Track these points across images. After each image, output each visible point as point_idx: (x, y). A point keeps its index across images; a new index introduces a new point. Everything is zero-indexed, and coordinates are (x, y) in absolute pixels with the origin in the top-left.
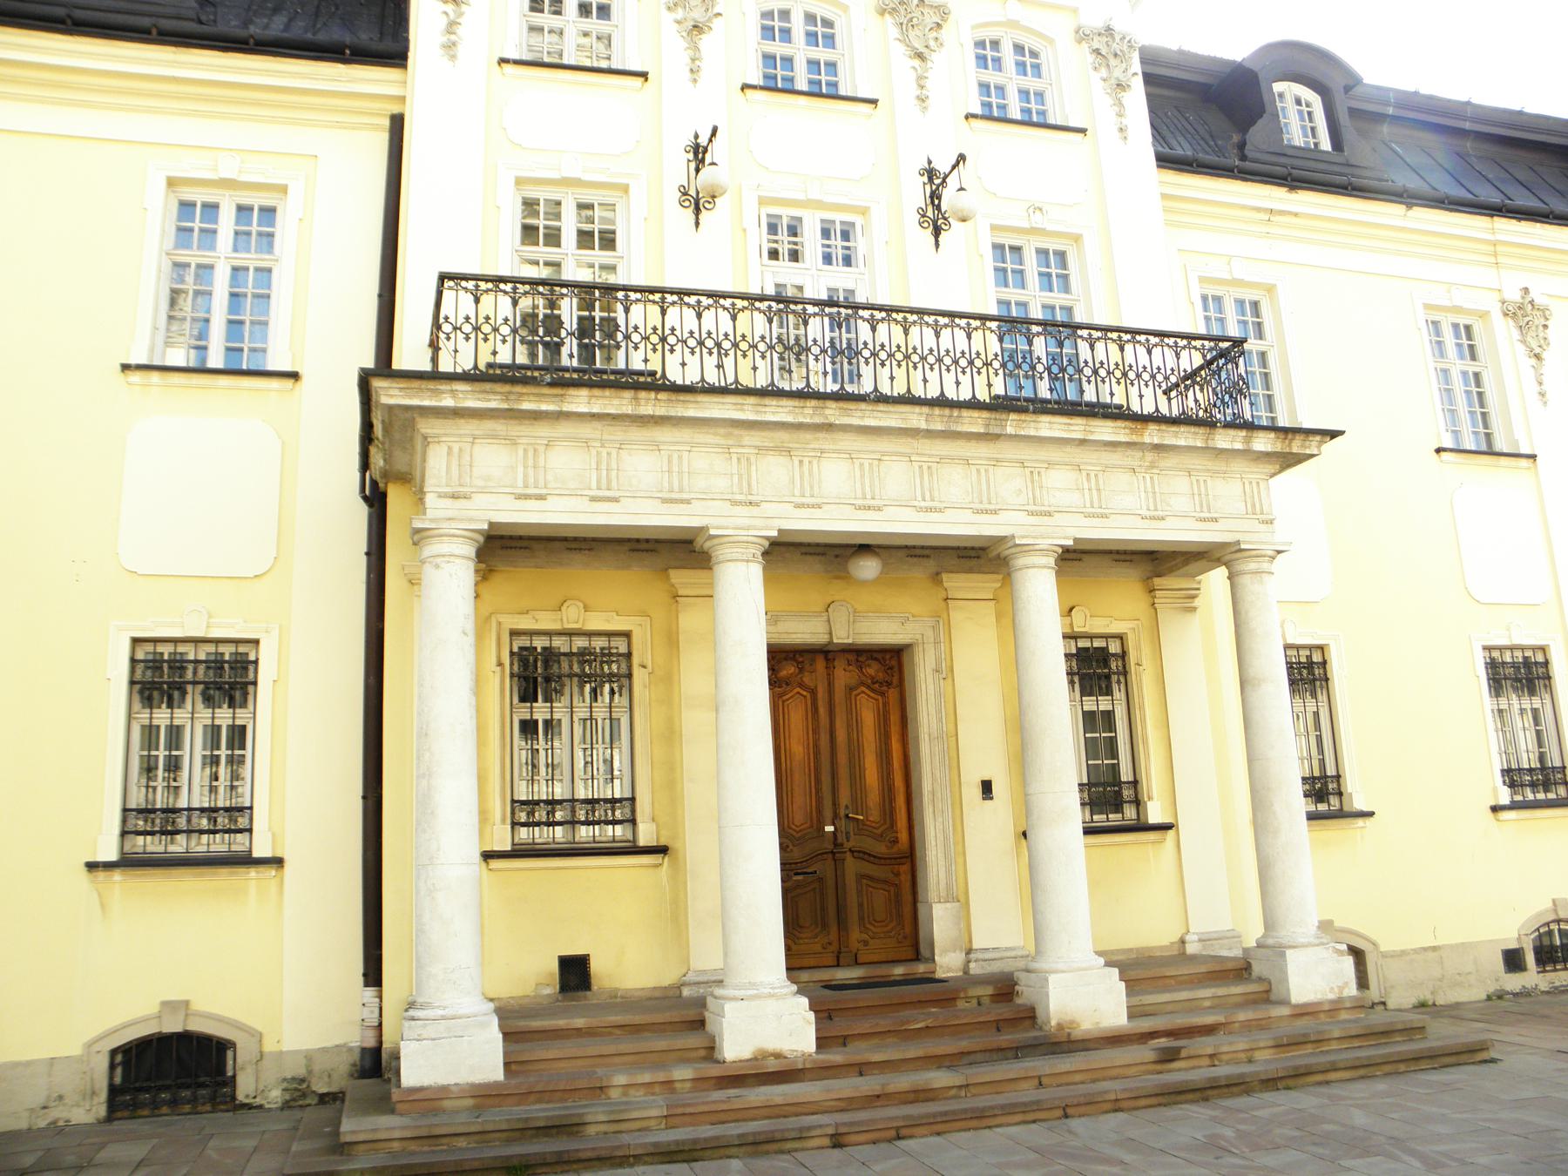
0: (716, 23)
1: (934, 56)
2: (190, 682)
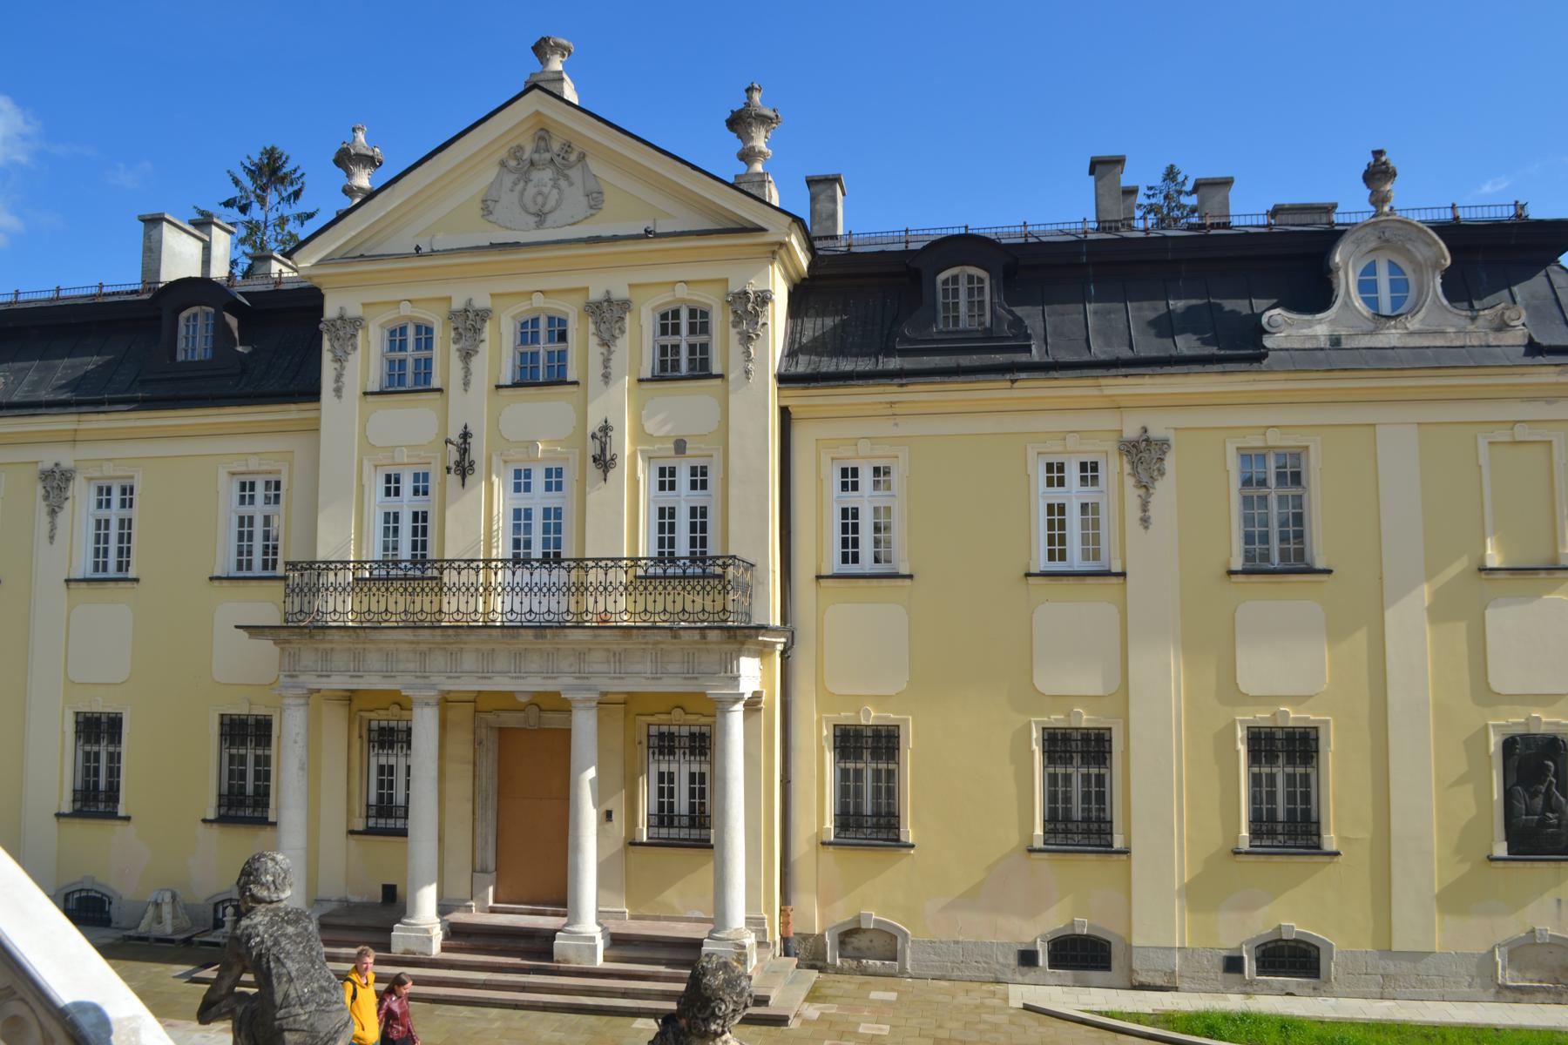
2: (246, 734)
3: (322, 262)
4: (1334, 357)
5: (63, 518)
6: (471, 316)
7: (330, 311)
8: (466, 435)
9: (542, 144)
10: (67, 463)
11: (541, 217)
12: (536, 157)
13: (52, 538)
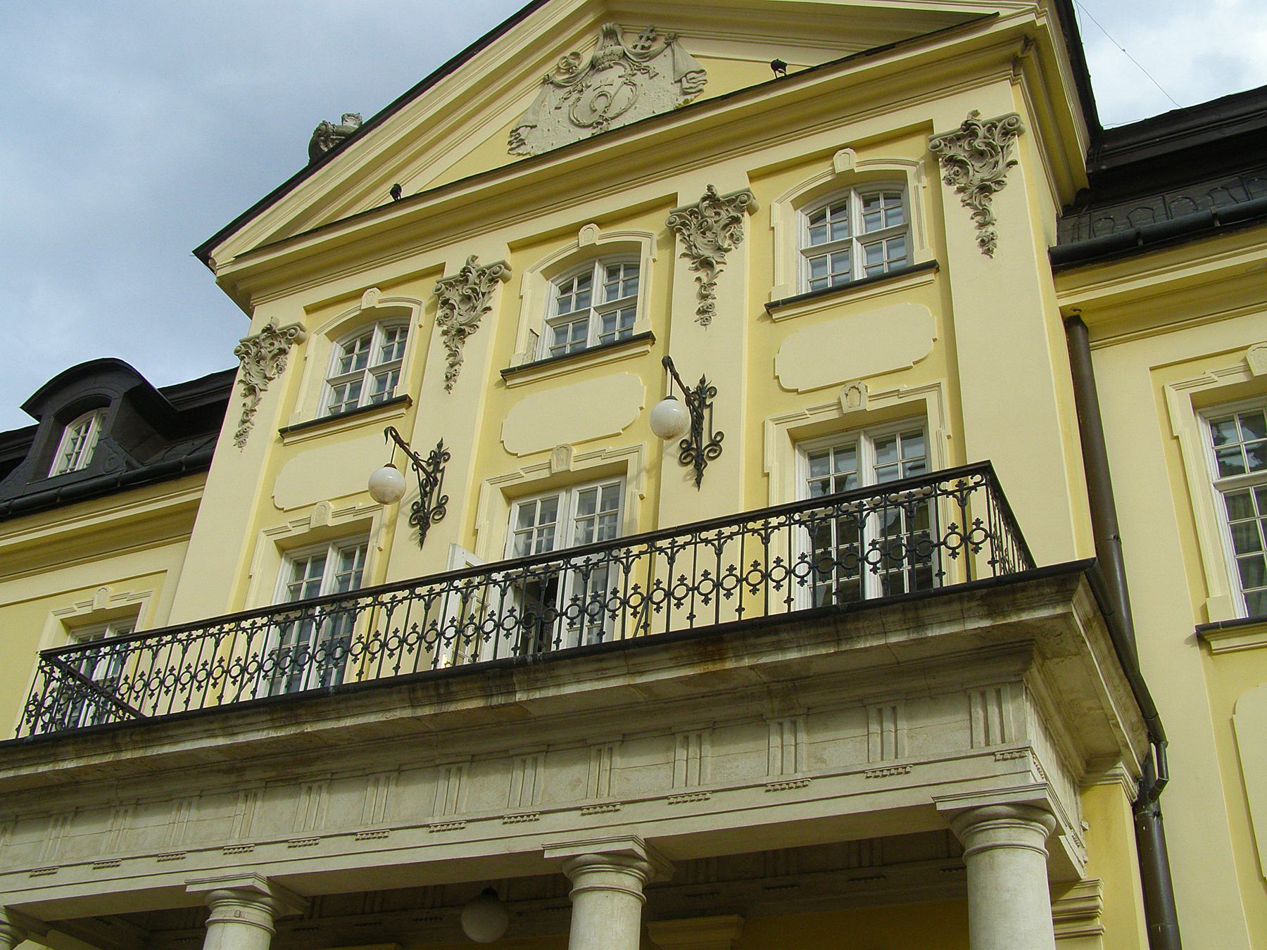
1: (728, 257)
8: (439, 456)
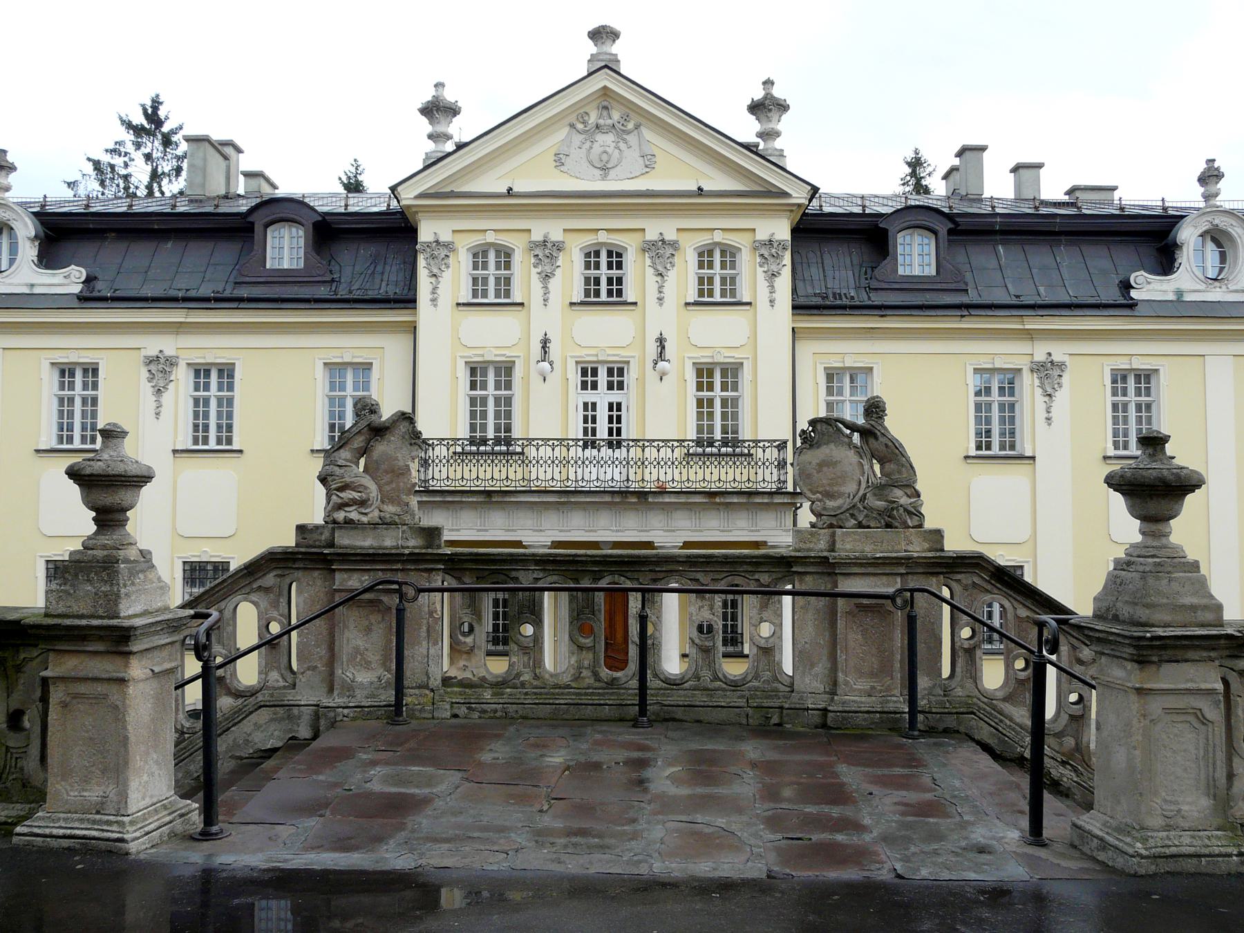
0: (558, 272)
3: (422, 196)
4: (1179, 309)
5: (167, 398)
6: (549, 245)
7: (426, 232)
9: (605, 113)
10: (169, 352)
11: (605, 170)
12: (601, 122)
13: (157, 414)
